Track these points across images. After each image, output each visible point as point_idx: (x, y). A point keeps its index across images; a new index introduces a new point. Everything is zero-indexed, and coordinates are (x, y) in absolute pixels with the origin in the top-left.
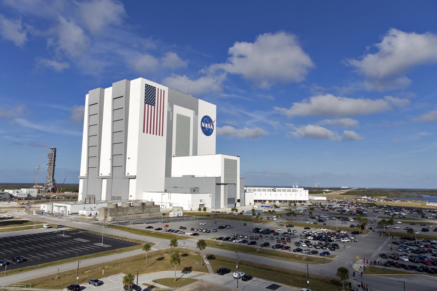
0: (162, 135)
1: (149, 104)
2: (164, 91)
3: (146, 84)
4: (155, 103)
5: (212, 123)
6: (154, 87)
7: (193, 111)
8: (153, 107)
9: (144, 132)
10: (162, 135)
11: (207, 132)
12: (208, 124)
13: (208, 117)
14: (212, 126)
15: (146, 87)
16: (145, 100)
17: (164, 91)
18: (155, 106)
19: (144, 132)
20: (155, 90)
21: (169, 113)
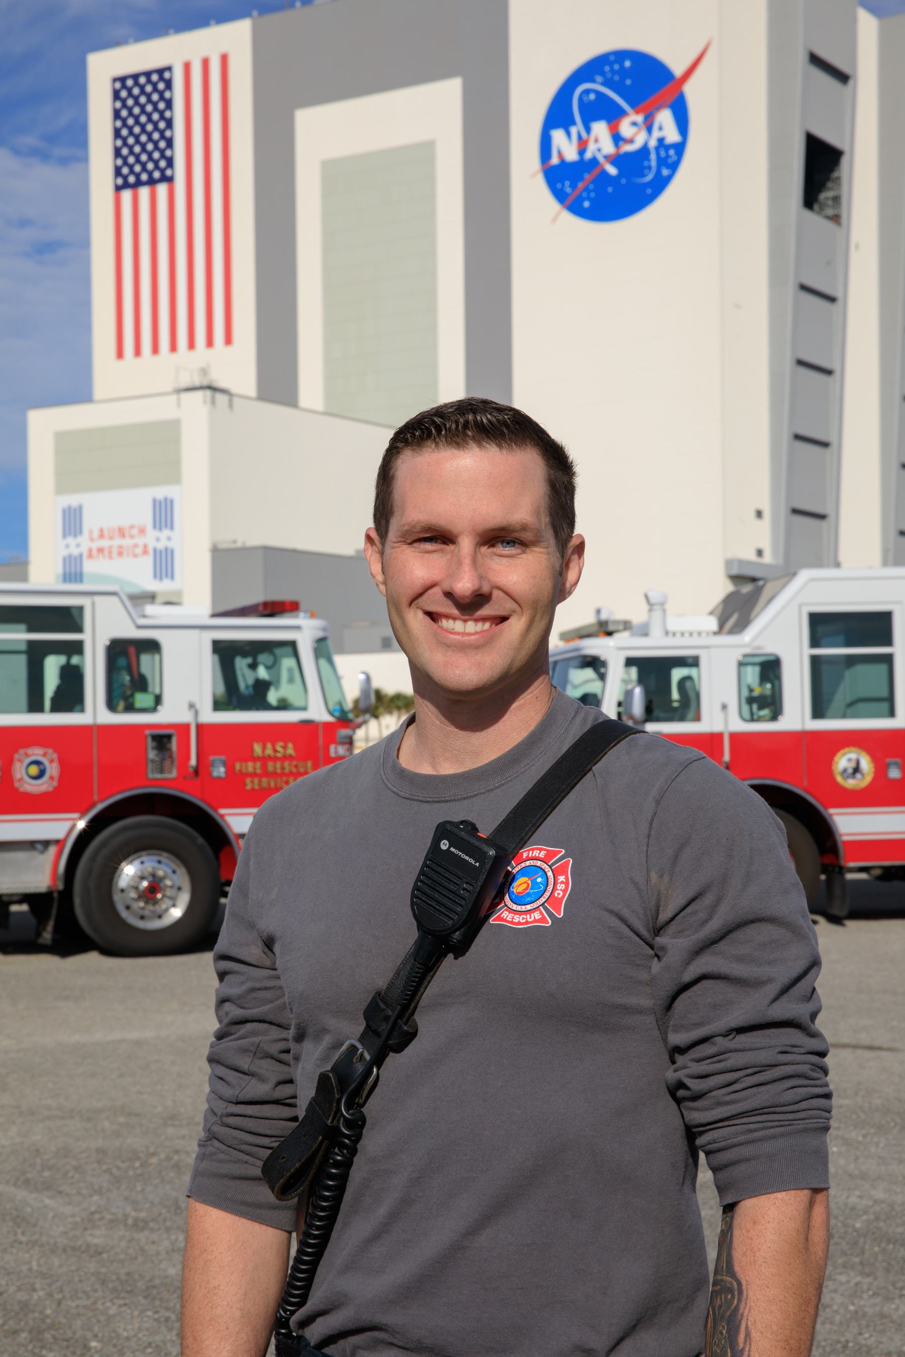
0: (228, 340)
2: (224, 59)
3: (115, 80)
6: (160, 72)
8: (162, 189)
9: (120, 354)
10: (228, 340)
11: (610, 192)
13: (621, 55)
14: (665, 118)
15: (116, 95)
16: (118, 172)
17: (224, 59)
18: (170, 180)
19: (120, 354)
20: (169, 84)
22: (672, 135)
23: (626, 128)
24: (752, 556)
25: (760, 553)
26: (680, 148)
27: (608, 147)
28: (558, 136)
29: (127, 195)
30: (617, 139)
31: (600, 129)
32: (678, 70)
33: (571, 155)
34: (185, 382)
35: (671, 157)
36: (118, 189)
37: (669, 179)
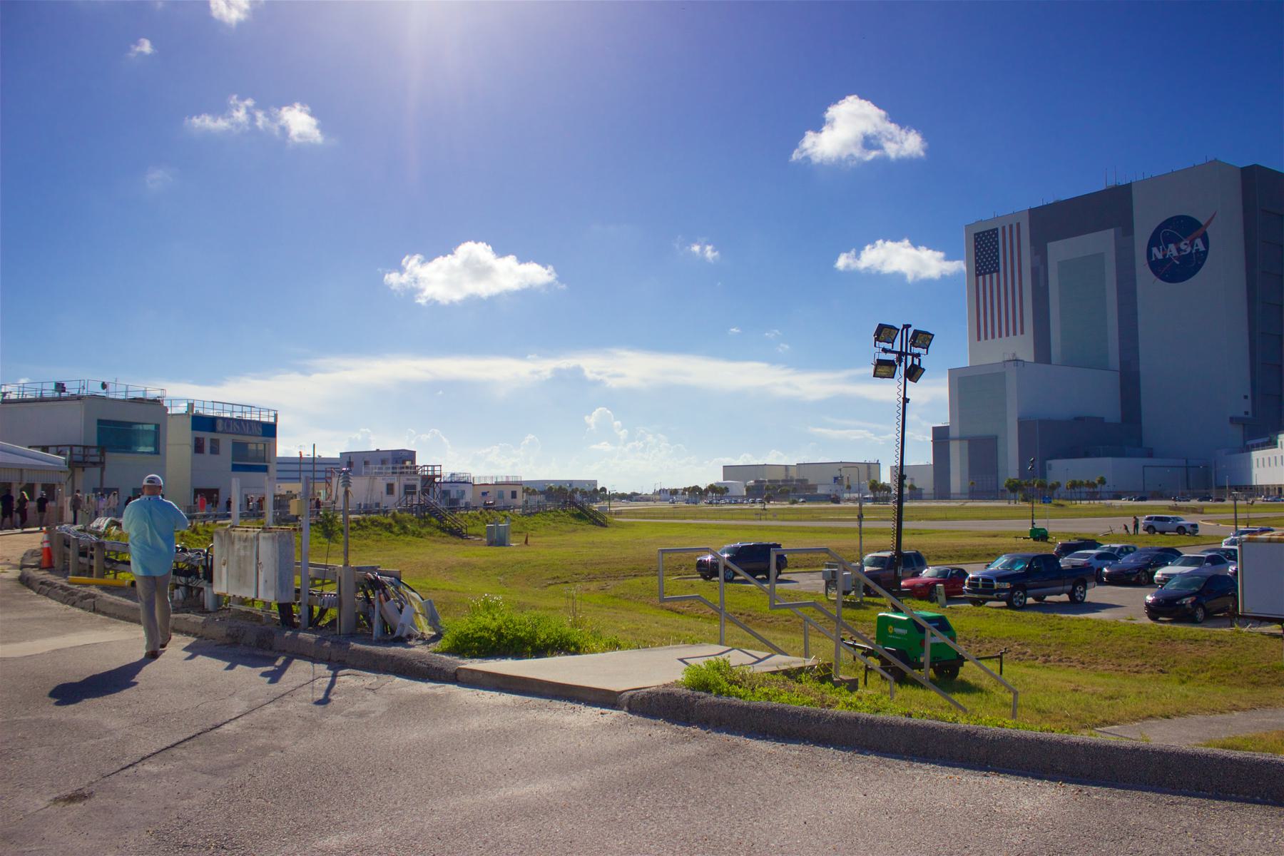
0: (1022, 333)
1: (984, 274)
2: (1018, 225)
4: (998, 264)
5: (1200, 232)
7: (1111, 232)
8: (995, 275)
9: (979, 339)
10: (1022, 333)
12: (1176, 241)
14: (1199, 241)
16: (977, 269)
17: (1018, 225)
18: (998, 271)
19: (979, 339)
20: (997, 235)
21: (1035, 272)
22: (1202, 248)
23: (1182, 246)
24: (1242, 415)
25: (1246, 413)
26: (1206, 253)
27: (1175, 253)
28: (1155, 250)
29: (981, 278)
30: (1179, 250)
31: (1172, 246)
32: (1203, 222)
33: (1160, 256)
34: (1007, 358)
35: (1200, 258)
36: (977, 276)
37: (1200, 266)
